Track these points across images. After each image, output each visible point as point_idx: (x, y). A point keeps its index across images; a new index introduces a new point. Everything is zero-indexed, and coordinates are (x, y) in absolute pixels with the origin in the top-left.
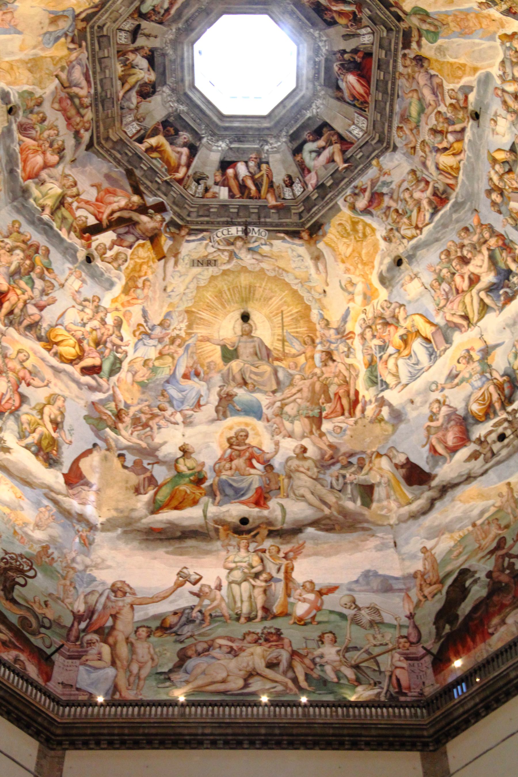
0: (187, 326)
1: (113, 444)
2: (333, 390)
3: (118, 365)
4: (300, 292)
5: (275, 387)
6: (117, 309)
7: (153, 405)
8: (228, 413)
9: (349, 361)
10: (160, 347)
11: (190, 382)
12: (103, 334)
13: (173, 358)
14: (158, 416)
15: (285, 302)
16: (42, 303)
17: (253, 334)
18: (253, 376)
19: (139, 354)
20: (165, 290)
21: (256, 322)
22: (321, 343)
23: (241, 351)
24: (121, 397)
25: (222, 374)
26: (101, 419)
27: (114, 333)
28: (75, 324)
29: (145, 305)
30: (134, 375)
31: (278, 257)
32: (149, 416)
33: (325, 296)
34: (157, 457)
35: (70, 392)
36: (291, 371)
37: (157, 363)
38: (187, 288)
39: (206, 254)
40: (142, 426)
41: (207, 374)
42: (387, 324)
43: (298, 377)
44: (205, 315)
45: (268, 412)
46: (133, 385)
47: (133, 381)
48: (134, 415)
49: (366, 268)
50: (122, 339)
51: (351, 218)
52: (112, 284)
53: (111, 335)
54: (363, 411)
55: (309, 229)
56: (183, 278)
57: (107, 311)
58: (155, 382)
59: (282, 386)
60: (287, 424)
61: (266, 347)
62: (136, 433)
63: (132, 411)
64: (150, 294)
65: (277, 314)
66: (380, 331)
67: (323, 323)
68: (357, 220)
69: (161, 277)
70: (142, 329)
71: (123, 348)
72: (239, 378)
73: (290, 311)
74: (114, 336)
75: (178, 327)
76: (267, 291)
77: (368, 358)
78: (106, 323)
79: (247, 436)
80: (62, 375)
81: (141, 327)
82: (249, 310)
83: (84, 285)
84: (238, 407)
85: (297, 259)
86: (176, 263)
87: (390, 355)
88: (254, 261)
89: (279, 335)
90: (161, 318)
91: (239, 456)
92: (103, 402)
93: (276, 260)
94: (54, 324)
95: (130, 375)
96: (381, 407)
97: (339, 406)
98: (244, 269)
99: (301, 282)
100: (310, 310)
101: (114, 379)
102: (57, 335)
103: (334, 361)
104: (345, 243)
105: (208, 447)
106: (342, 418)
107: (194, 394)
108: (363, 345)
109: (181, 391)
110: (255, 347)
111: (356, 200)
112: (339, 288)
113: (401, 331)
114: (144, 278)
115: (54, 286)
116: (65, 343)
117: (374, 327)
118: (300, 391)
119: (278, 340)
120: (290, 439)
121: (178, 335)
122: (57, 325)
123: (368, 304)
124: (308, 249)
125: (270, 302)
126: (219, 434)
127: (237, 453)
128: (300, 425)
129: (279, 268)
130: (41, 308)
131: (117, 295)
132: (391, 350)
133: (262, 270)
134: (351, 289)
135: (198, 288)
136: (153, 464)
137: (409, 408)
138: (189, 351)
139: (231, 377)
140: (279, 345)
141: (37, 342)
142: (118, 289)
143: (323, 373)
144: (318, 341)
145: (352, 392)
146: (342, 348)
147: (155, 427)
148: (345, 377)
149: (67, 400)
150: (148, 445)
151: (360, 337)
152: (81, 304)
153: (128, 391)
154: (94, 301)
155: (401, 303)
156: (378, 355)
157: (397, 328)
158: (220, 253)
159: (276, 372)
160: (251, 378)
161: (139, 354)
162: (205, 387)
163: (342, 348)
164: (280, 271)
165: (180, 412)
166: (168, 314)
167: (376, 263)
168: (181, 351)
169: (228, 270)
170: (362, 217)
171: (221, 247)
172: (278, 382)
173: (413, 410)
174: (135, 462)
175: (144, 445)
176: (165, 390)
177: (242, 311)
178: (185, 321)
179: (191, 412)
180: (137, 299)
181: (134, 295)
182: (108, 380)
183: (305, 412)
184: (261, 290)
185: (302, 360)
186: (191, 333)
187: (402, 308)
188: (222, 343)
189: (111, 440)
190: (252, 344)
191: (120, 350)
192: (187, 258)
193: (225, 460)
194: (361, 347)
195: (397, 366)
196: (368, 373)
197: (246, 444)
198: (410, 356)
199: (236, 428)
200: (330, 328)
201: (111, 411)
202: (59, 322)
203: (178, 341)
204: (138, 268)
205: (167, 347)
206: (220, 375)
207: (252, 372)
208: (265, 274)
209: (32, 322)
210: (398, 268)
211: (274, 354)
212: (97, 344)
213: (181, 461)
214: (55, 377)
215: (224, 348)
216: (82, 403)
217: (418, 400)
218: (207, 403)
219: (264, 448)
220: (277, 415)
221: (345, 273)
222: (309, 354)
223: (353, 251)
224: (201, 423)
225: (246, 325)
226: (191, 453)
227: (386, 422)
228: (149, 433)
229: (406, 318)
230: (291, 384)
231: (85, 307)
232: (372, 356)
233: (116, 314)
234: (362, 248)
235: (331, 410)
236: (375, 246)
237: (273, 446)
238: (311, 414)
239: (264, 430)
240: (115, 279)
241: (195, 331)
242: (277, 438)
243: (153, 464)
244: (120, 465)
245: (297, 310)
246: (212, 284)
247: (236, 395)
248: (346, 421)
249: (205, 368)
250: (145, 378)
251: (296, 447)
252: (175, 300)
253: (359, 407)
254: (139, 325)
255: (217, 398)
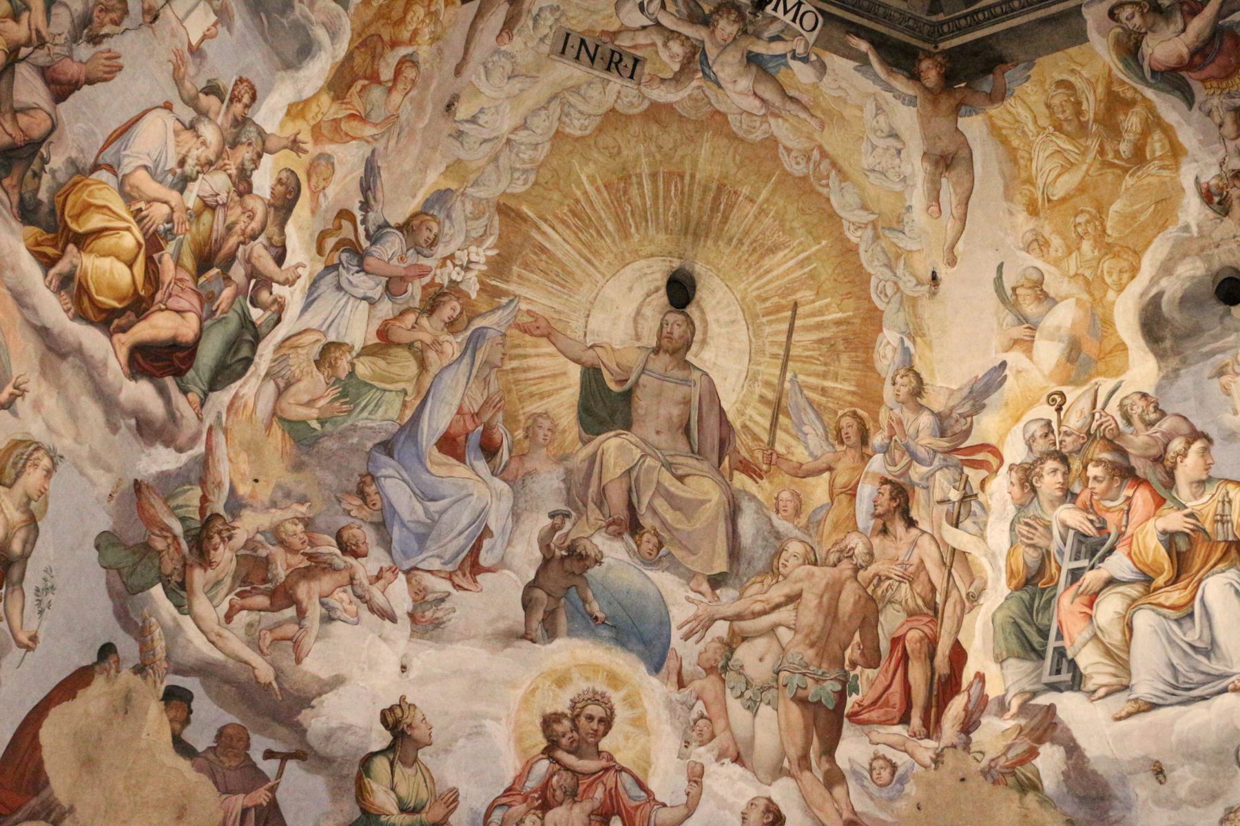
0: (489, 261)
1: (160, 645)
2: (890, 622)
3: (245, 352)
4: (864, 258)
5: (721, 565)
6: (295, 145)
7: (321, 522)
8: (562, 620)
9: (958, 538)
10: (386, 309)
11: (461, 471)
12: (229, 229)
13: (423, 365)
14: (330, 568)
15: (812, 276)
16: (71, 70)
17: (690, 357)
18: (661, 504)
19: (313, 319)
20: (449, 106)
21: (710, 317)
22: (886, 450)
23: (643, 402)
24: (223, 470)
25: (569, 472)
26: (147, 547)
27: (263, 229)
28: (153, 176)
29: (380, 146)
30: (280, 393)
31: (829, 118)
32: (300, 562)
33: (933, 294)
34: (301, 731)
35: (77, 439)
36: (781, 524)
37: (364, 369)
38: (524, 126)
39: (614, 27)
40: (272, 594)
41: (522, 456)
42: (1125, 473)
43: (795, 547)
44: (558, 241)
45: (685, 651)
46: (269, 427)
47: (274, 414)
48: (250, 544)
49: (1106, 265)
50: (280, 259)
51: (1110, 80)
52: (306, 50)
53: (254, 237)
54: (968, 725)
55: (948, 53)
56: (516, 85)
57: (264, 146)
58: (342, 436)
59: (743, 567)
60: (736, 709)
61: (722, 412)
62: (243, 617)
63: (248, 525)
64: (407, 111)
65: (778, 309)
66: (1100, 487)
67: (906, 384)
68: (1129, 95)
69: (453, 62)
70: (347, 230)
71: (276, 288)
72: (616, 498)
73: (821, 312)
74: (262, 239)
75: (462, 257)
76: (767, 221)
77: (1032, 556)
78: (249, 190)
79: (607, 722)
80: (67, 369)
81: (346, 224)
82: (699, 268)
83: (222, 30)
84: (595, 608)
85: (882, 143)
86: (509, 25)
87: (1111, 582)
88: (753, 104)
89: (767, 384)
90: (414, 205)
91: (573, 795)
92: (169, 483)
93: (822, 126)
94: (91, 160)
95: (270, 388)
96: (1040, 741)
97: (897, 686)
98: (717, 121)
99: (874, 225)
100: (881, 330)
101: (222, 398)
102: (88, 207)
103: (911, 523)
104: (1060, 151)
105: (477, 733)
106: (899, 729)
107: (465, 520)
108: (1021, 507)
109: (426, 496)
110: (687, 402)
111: (1151, 29)
112: (991, 288)
113: (1174, 520)
114: (403, 51)
115: (126, 12)
116: (106, 242)
117: (1076, 465)
118: (793, 599)
119: (762, 399)
120: (737, 768)
121: (452, 281)
122: (96, 167)
123: (1076, 383)
124: (924, 122)
125: (767, 262)
126: (519, 693)
127: (566, 779)
128: (775, 725)
129: (824, 154)
130: (62, 89)
131: (308, 93)
132: (1118, 564)
133: (772, 142)
134: (1030, 309)
135: (559, 135)
136: (285, 757)
137: (1142, 789)
138: (480, 357)
139: (593, 490)
140: (760, 420)
141: (16, 225)
142: (318, 70)
143: (871, 554)
144: (877, 440)
145: (943, 648)
146: (945, 486)
147: (315, 612)
148: (933, 590)
149: (61, 467)
150: (279, 674)
151: (1015, 477)
152: (192, 102)
153: (253, 449)
154: (234, 99)
155: (1199, 428)
156: (1067, 565)
157: (1160, 502)
158: (659, 43)
159: (733, 513)
160: (655, 512)
161: (313, 319)
162: (506, 504)
163: (945, 486)
164: (825, 165)
165: (407, 572)
166: (441, 198)
167: (1149, 263)
168: (453, 345)
169: (669, 107)
170: (1150, 93)
171: (666, 21)
172: (734, 553)
173: (1158, 802)
174: (221, 733)
175: (265, 672)
176: (374, 479)
177: (676, 264)
178: (491, 241)
179: (441, 586)
180: (363, 119)
181: (358, 105)
182: (202, 405)
183: (797, 679)
184: (752, 210)
185: (818, 489)
186: (496, 293)
187: (1198, 445)
188: (589, 357)
189: (157, 632)
190: (682, 391)
191: (264, 296)
192: (548, 19)
193: (525, 800)
194: (1011, 510)
195: (1130, 628)
196: (1015, 608)
197: (599, 753)
198: (1185, 614)
199: (579, 686)
200: (920, 408)
201: (183, 520)
202: (108, 157)
203: (450, 309)
204: (396, 14)
205: (410, 319)
206: (560, 471)
207: (661, 491)
208: (776, 158)
209: (19, 138)
210: (1221, 308)
211: (743, 444)
212: (204, 261)
213: (381, 766)
214: (43, 373)
215: (592, 376)
216: (105, 483)
217: (1185, 778)
218: (502, 564)
219: (653, 784)
220: (710, 670)
221: (1027, 249)
222: (841, 480)
223: (1081, 189)
224: (465, 637)
225: (674, 317)
226: (419, 745)
227: (1045, 801)
228: (291, 629)
229: (1202, 483)
230: (773, 570)
231: (202, 113)
232: (1046, 556)
233: (288, 159)
234: (1114, 196)
235: (872, 696)
236: (1166, 205)
237: (682, 782)
238: (812, 691)
239: (665, 714)
240: (321, 34)
241: (512, 288)
242: (702, 754)
243: (285, 757)
244: (167, 737)
245: (839, 315)
246: (606, 140)
247: (598, 562)
248: (910, 745)
249: (520, 434)
250: (314, 413)
251: (752, 803)
252: (475, 155)
253: (956, 706)
254: (344, 214)
255: (538, 555)
